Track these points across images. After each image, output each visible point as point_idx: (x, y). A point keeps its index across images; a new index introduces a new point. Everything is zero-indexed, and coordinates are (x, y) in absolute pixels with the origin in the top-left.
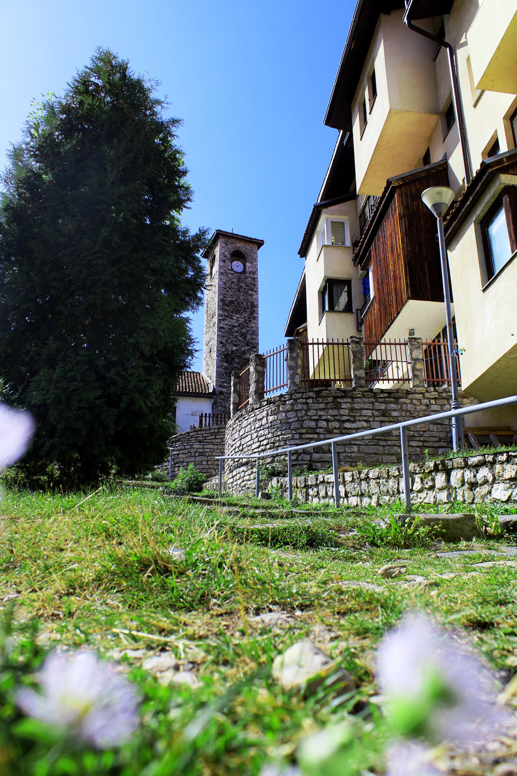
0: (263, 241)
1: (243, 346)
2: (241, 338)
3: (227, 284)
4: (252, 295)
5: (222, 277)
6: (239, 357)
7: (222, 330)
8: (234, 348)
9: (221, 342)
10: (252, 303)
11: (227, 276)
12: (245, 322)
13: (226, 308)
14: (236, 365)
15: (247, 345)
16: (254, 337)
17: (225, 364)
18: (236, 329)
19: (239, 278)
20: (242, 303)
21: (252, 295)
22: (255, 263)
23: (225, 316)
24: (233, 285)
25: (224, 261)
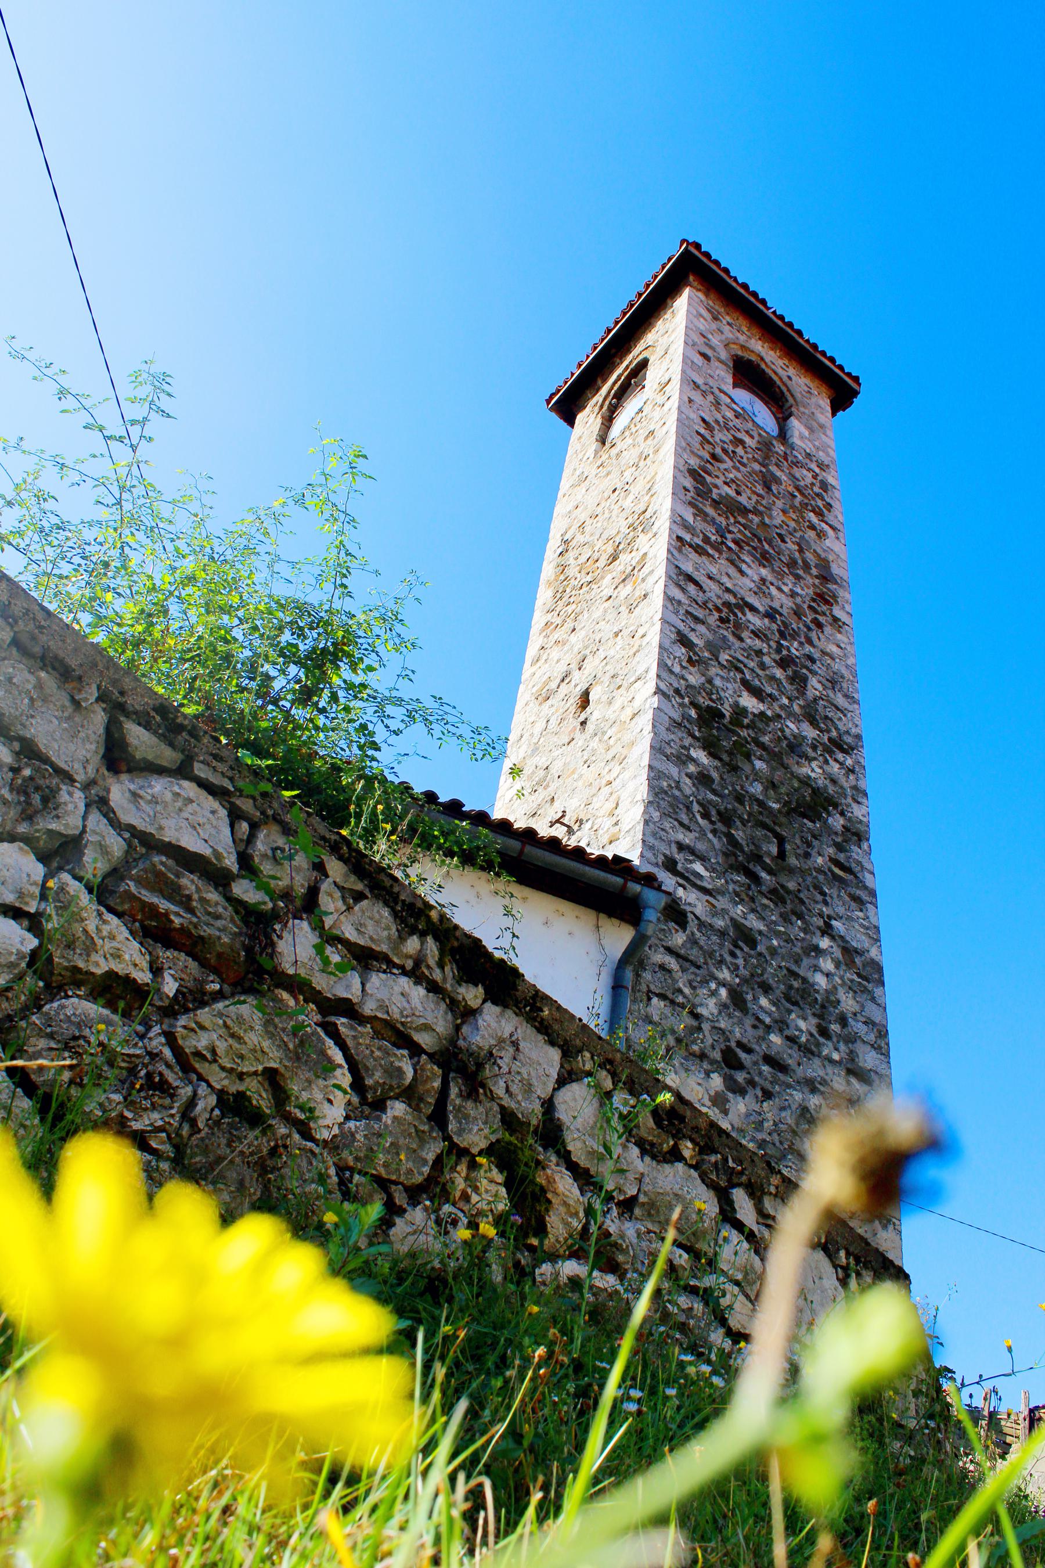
0: (856, 379)
1: (791, 715)
2: (779, 673)
6: (775, 758)
7: (691, 588)
8: (749, 702)
9: (683, 640)
10: (824, 565)
12: (798, 613)
15: (811, 717)
16: (840, 700)
17: (700, 755)
18: (756, 621)
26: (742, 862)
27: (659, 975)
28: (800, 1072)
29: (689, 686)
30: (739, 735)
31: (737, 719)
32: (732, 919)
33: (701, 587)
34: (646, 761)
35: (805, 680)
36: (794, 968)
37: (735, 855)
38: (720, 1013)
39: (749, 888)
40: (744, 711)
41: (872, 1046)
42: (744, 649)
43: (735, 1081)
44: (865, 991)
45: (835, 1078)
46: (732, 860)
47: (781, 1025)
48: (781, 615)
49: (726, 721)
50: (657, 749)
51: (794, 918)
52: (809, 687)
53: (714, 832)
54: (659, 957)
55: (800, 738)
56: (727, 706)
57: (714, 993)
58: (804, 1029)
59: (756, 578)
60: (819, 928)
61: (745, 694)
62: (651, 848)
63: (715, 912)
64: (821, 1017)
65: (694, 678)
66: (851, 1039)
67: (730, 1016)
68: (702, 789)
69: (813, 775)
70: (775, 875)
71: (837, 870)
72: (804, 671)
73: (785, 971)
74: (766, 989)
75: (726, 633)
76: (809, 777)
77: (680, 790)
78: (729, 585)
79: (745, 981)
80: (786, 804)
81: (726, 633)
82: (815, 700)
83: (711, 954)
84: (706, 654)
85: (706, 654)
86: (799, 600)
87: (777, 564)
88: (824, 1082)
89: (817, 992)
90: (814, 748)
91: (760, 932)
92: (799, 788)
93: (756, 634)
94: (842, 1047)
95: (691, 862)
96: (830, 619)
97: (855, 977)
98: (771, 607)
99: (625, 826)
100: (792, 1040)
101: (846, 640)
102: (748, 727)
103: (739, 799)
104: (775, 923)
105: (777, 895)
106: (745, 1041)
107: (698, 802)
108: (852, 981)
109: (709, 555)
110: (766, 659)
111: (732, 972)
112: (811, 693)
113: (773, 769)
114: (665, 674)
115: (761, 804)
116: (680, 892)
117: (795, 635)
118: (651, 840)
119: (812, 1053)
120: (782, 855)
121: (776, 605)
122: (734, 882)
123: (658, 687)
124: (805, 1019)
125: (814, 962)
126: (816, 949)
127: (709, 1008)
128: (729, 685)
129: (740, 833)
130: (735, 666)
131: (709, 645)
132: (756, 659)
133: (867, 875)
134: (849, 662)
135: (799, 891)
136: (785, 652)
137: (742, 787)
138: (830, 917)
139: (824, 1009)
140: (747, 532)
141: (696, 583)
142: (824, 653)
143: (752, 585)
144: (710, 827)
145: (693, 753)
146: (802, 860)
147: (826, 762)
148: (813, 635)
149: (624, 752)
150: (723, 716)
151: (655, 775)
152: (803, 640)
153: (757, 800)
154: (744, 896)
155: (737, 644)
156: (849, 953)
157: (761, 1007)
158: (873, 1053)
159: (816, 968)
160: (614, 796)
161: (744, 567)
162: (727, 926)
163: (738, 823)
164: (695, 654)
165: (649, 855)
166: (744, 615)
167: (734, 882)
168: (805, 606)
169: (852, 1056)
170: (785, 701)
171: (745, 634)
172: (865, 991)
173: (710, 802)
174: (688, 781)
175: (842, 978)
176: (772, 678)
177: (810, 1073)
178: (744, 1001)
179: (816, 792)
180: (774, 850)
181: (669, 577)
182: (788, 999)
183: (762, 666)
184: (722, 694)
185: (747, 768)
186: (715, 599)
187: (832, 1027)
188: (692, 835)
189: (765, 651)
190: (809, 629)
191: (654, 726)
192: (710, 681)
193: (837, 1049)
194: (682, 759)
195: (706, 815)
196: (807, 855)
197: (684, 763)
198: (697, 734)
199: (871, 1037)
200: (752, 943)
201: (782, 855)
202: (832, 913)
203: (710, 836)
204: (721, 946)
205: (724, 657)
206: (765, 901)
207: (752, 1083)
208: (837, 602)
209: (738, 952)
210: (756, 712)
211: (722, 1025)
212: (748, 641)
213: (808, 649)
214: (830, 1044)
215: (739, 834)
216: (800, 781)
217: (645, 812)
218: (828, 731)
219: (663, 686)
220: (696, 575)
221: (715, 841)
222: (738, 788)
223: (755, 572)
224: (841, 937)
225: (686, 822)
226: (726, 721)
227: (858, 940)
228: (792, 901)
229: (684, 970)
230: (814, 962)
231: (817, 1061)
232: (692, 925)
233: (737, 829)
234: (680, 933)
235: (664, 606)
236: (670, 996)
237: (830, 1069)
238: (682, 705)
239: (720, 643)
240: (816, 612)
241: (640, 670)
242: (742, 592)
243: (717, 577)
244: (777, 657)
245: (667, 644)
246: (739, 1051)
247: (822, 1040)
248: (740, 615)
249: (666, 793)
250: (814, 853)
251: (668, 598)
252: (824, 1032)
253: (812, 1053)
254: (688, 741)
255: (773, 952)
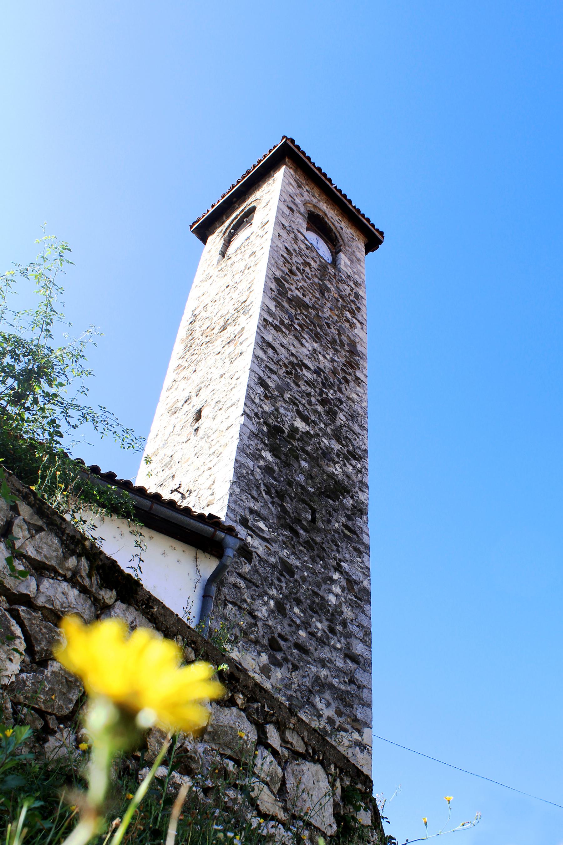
1: (325, 434)
2: (320, 408)
3: (295, 259)
4: (352, 326)
5: (284, 233)
7: (270, 351)
8: (300, 425)
9: (262, 383)
10: (353, 344)
11: (296, 239)
12: (334, 372)
13: (286, 305)
14: (301, 478)
15: (337, 436)
16: (356, 428)
17: (267, 455)
18: (308, 375)
19: (323, 268)
20: (329, 327)
21: (352, 326)
22: (359, 266)
23: (282, 322)
24: (307, 269)
25: (290, 209)
26: (288, 523)
27: (232, 590)
28: (316, 654)
29: (264, 412)
30: (292, 445)
31: (292, 434)
32: (280, 558)
33: (276, 351)
34: (233, 456)
35: (335, 413)
36: (316, 590)
37: (285, 519)
38: (269, 616)
39: (292, 540)
40: (296, 430)
41: (361, 640)
42: (300, 392)
43: (276, 658)
44: (359, 606)
45: (338, 659)
46: (282, 521)
47: (306, 625)
48: (324, 373)
49: (285, 435)
50: (241, 449)
51: (318, 560)
52: (338, 418)
53: (273, 503)
54: (233, 579)
55: (329, 449)
56: (286, 426)
57: (266, 603)
58: (320, 628)
59: (310, 349)
60: (333, 566)
61: (298, 419)
62: (233, 511)
63: (269, 553)
64: (331, 621)
65: (267, 408)
66: (348, 635)
67: (275, 618)
68: (267, 476)
69: (336, 472)
70: (308, 532)
71: (346, 532)
72: (336, 408)
73: (311, 592)
74: (298, 602)
75: (289, 381)
76: (334, 473)
77: (253, 476)
78: (294, 352)
79: (286, 597)
80: (318, 489)
81: (289, 381)
82: (341, 426)
83: (266, 579)
84: (276, 393)
85: (276, 393)
86: (335, 364)
87: (324, 341)
88: (331, 661)
89: (330, 605)
90: (338, 456)
91: (297, 567)
92: (327, 480)
93: (307, 383)
94: (343, 640)
95: (257, 521)
96: (353, 378)
97: (353, 598)
98: (318, 367)
99: (217, 496)
100: (312, 634)
101: (362, 391)
102: (298, 440)
103: (290, 484)
104: (306, 561)
105: (309, 545)
106: (283, 633)
107: (264, 484)
108: (351, 600)
109: (285, 333)
110: (313, 399)
111: (278, 591)
112: (338, 422)
113: (312, 467)
114: (249, 404)
115: (303, 488)
116: (249, 539)
117: (331, 386)
118: (233, 506)
119: (324, 643)
120: (314, 520)
121: (321, 366)
122: (283, 535)
123: (244, 411)
124: (321, 622)
125: (329, 587)
126: (331, 579)
127: (262, 612)
128: (289, 413)
129: (289, 505)
130: (293, 401)
131: (278, 387)
132: (307, 399)
133: (365, 536)
134: (363, 405)
135: (323, 543)
136: (324, 396)
137: (292, 477)
138: (340, 560)
139: (333, 616)
140: (307, 320)
141: (273, 349)
142: (348, 398)
143: (308, 353)
144: (271, 500)
145: (263, 454)
146: (326, 524)
147: (345, 465)
148: (343, 387)
149: (221, 450)
150: (284, 432)
151: (239, 466)
152: (336, 389)
153: (301, 485)
154: (288, 544)
155: (296, 388)
156: (351, 584)
157: (295, 613)
158: (361, 645)
159: (330, 591)
160: (213, 477)
161: (304, 341)
162: (276, 562)
163: (288, 499)
164: (269, 392)
165: (231, 515)
166: (302, 370)
167: (283, 535)
168: (339, 369)
169: (349, 646)
170: (323, 426)
171: (301, 383)
172: (359, 606)
173: (272, 484)
174: (259, 470)
175: (345, 598)
176: (315, 411)
177: (322, 655)
178: (285, 609)
179: (337, 483)
180: (309, 517)
181: (257, 343)
182: (312, 609)
183: (310, 403)
184: (284, 418)
185: (296, 466)
186: (284, 359)
187: (338, 627)
188: (259, 504)
189: (312, 394)
190: (341, 383)
191: (240, 435)
192: (277, 410)
193: (339, 641)
194: (256, 457)
195: (268, 493)
196: (329, 521)
197: (257, 459)
198: (266, 442)
199: (361, 635)
200: (292, 573)
201: (314, 520)
202: (342, 558)
203: (270, 506)
204: (273, 574)
205: (287, 396)
206: (301, 548)
207: (286, 660)
208: (359, 368)
209: (283, 579)
210: (304, 431)
211: (270, 623)
212: (303, 387)
213: (339, 395)
214: (336, 638)
215: (288, 506)
216: (328, 476)
217: (231, 488)
218: (347, 446)
219: (248, 411)
220: (274, 344)
221: (273, 509)
222: (290, 477)
223: (310, 345)
224: (347, 573)
225: (256, 496)
226: (285, 435)
227: (357, 575)
228: (318, 549)
229: (248, 588)
230: (329, 587)
231: (327, 648)
232: (255, 560)
233: (287, 503)
234: (247, 565)
235: (253, 361)
236: (239, 604)
237: (334, 654)
238: (259, 423)
239: (285, 387)
240: (346, 373)
241: (234, 400)
242: (301, 356)
243: (287, 346)
244: (320, 399)
245: (252, 385)
246: (279, 639)
247: (330, 635)
248: (299, 370)
249: (245, 477)
250: (333, 520)
251: (256, 357)
252: (332, 630)
253: (324, 643)
254: (260, 446)
255: (304, 579)
